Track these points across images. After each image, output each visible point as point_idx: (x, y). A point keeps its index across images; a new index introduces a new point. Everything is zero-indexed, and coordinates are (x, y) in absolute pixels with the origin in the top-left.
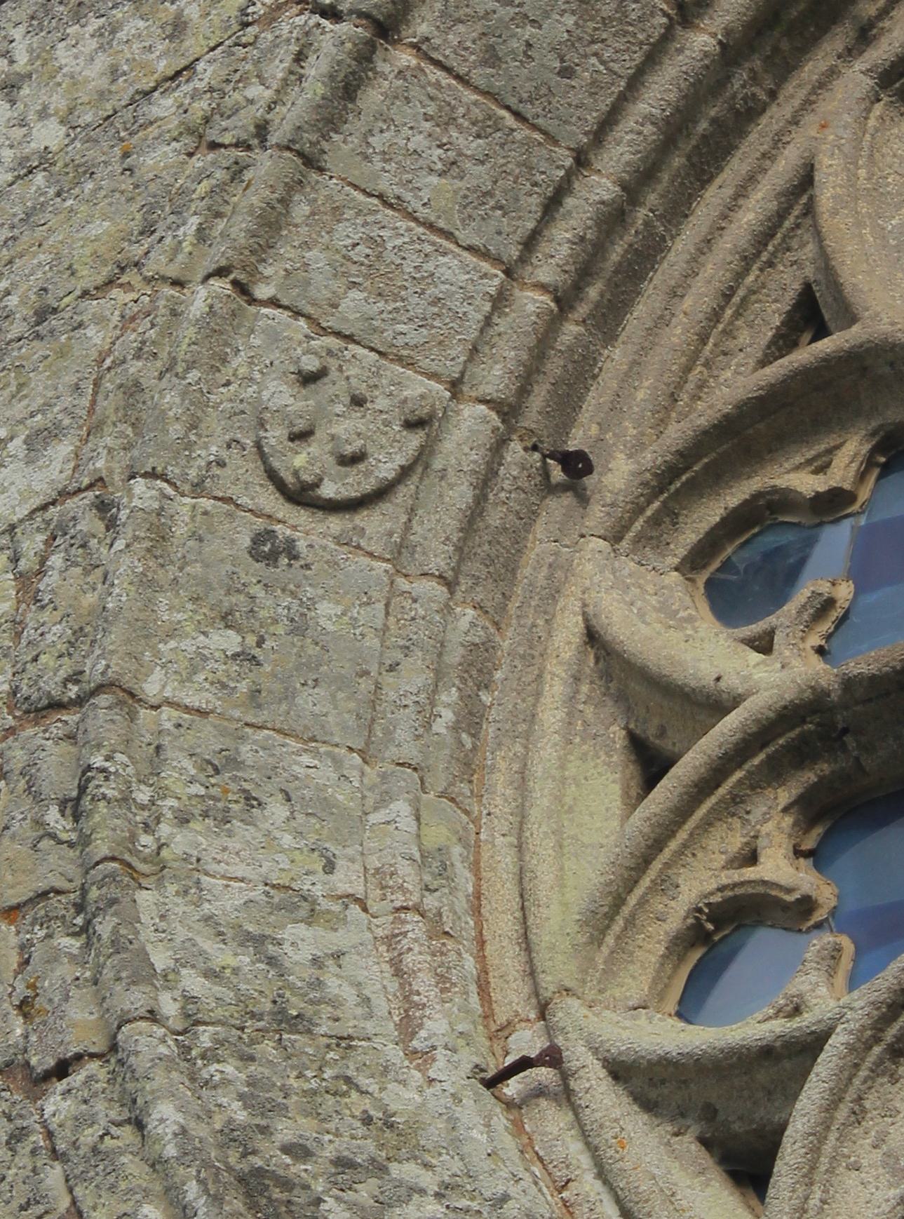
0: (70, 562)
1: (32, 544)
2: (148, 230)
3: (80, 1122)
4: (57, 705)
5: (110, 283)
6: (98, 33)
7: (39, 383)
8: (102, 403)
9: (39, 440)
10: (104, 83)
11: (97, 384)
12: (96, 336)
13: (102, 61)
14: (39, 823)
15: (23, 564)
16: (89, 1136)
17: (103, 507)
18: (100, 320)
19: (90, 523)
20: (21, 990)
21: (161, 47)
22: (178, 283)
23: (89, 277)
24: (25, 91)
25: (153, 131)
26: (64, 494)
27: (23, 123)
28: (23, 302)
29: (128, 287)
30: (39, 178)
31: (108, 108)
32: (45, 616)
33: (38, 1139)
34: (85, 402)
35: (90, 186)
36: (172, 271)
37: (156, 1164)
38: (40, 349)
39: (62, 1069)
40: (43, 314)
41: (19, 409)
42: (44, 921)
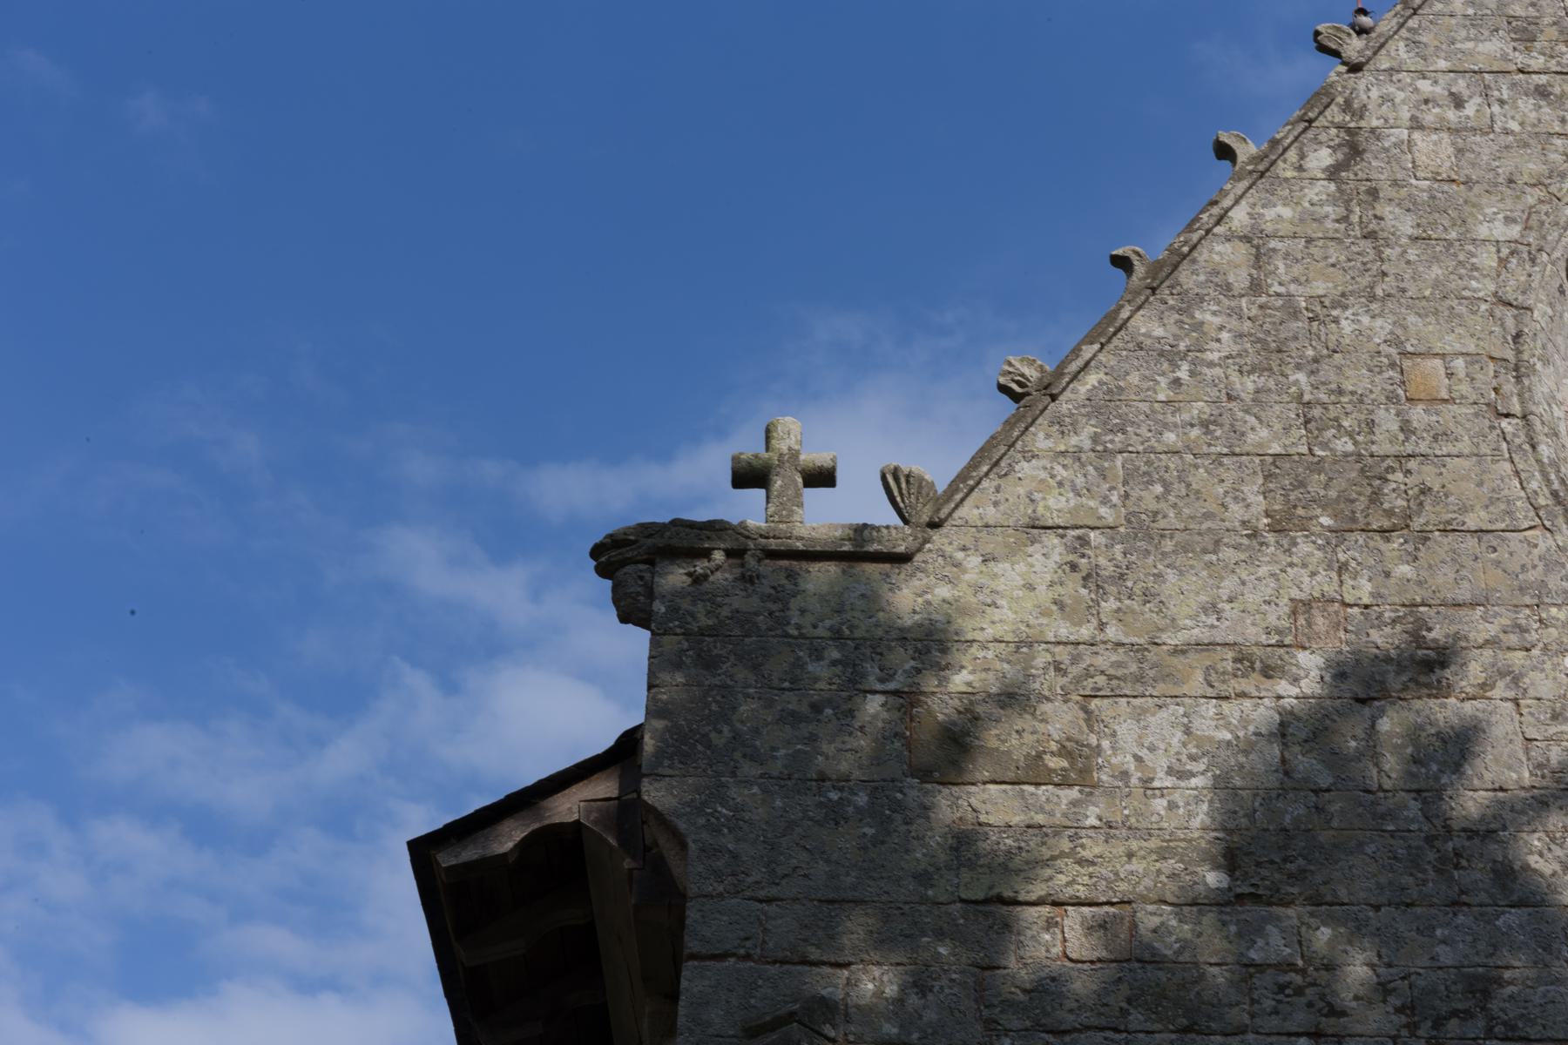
0: (1518, 264)
1: (1505, 251)
2: (1550, 177)
3: (1514, 435)
4: (1511, 305)
5: (1535, 185)
6: (1535, 104)
7: (1509, 201)
8: (1531, 222)
9: (1509, 220)
10: (1536, 122)
11: (1530, 214)
12: (1531, 200)
13: (1534, 115)
14: (1504, 338)
15: (1501, 255)
16: (1517, 441)
17: (1530, 253)
18: (1532, 195)
19: (1525, 256)
20: (1494, 383)
21: (1557, 123)
22: (1559, 199)
23: (1526, 178)
24: (1506, 107)
25: (1553, 147)
26: (1516, 242)
27: (1505, 116)
28: (1504, 173)
29: (1541, 191)
30: (1511, 138)
31: (1537, 130)
32: (1509, 275)
33: (1499, 431)
34: (1525, 217)
35: (1529, 151)
36: (1558, 195)
37: (1538, 461)
38: (1509, 192)
39: (1507, 416)
40: (1511, 181)
41: (1501, 206)
42: (1506, 368)
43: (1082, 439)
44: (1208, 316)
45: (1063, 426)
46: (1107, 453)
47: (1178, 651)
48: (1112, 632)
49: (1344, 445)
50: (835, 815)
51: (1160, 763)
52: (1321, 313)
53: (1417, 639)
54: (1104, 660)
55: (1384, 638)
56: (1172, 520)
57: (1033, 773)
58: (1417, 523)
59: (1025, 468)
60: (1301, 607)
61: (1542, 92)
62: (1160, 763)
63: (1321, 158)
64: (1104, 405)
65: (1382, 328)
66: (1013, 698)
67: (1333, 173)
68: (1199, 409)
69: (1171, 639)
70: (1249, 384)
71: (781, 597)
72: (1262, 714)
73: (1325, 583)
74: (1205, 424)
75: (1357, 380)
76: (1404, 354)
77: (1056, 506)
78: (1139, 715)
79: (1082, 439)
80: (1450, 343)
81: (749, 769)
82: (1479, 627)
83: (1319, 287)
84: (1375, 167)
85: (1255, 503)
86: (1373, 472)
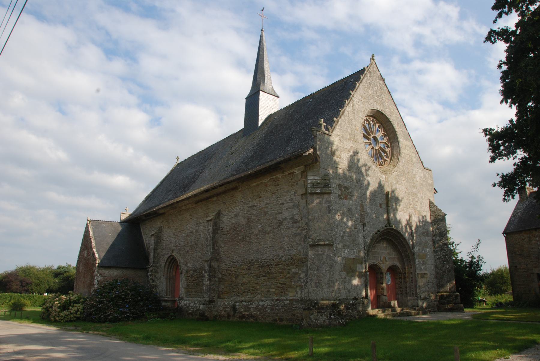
43: (339, 128)
44: (346, 118)
45: (339, 127)
46: (341, 130)
47: (345, 149)
48: (342, 146)
49: (353, 133)
50: (328, 158)
51: (344, 158)
52: (352, 120)
53: (357, 150)
54: (342, 148)
55: (355, 151)
56: (344, 137)
57: (338, 157)
58: (357, 141)
59: (337, 129)
60: (351, 147)
61: (363, 103)
62: (344, 158)
63: (351, 105)
64: (341, 124)
65: (355, 122)
66: (337, 150)
67: (352, 106)
68: (345, 127)
69: (345, 147)
70: (348, 125)
71: (324, 137)
72: (349, 155)
73: (352, 145)
74: (346, 128)
75: (354, 127)
76: (356, 126)
77: (338, 133)
78: (343, 153)
79: (339, 128)
80: (358, 125)
81: (323, 153)
82: (360, 151)
83: (352, 118)
84: (354, 107)
85: (348, 137)
86: (355, 136)
